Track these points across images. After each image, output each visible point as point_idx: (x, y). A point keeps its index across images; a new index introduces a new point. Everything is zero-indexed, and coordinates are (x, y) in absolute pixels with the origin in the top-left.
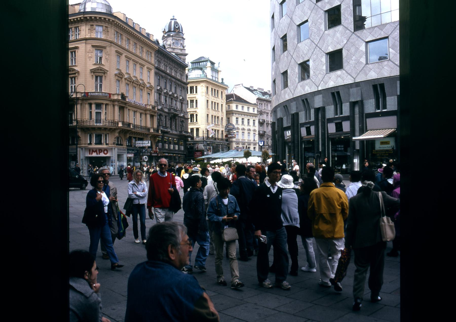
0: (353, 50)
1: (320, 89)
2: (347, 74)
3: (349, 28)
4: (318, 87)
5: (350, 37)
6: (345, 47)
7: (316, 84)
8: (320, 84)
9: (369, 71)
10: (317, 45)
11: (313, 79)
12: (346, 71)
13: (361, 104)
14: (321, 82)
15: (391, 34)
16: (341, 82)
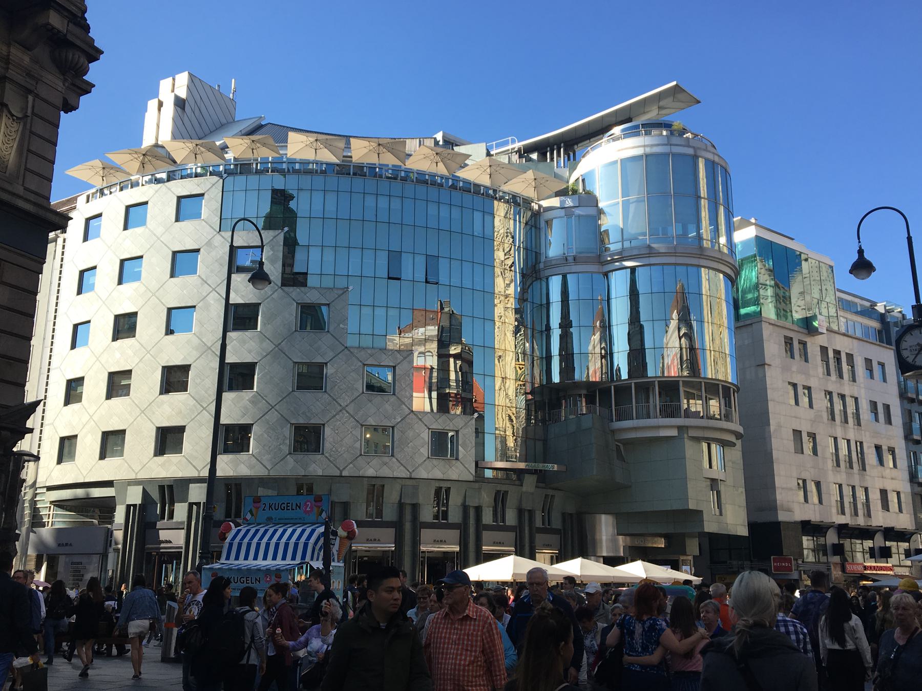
0: (410, 434)
1: (345, 473)
2: (398, 464)
3: (406, 404)
4: (341, 472)
5: (406, 416)
6: (398, 426)
7: (338, 466)
8: (347, 466)
9: (433, 469)
10: (344, 408)
11: (331, 456)
12: (397, 459)
13: (415, 507)
14: (349, 464)
15: (461, 428)
16: (386, 472)
